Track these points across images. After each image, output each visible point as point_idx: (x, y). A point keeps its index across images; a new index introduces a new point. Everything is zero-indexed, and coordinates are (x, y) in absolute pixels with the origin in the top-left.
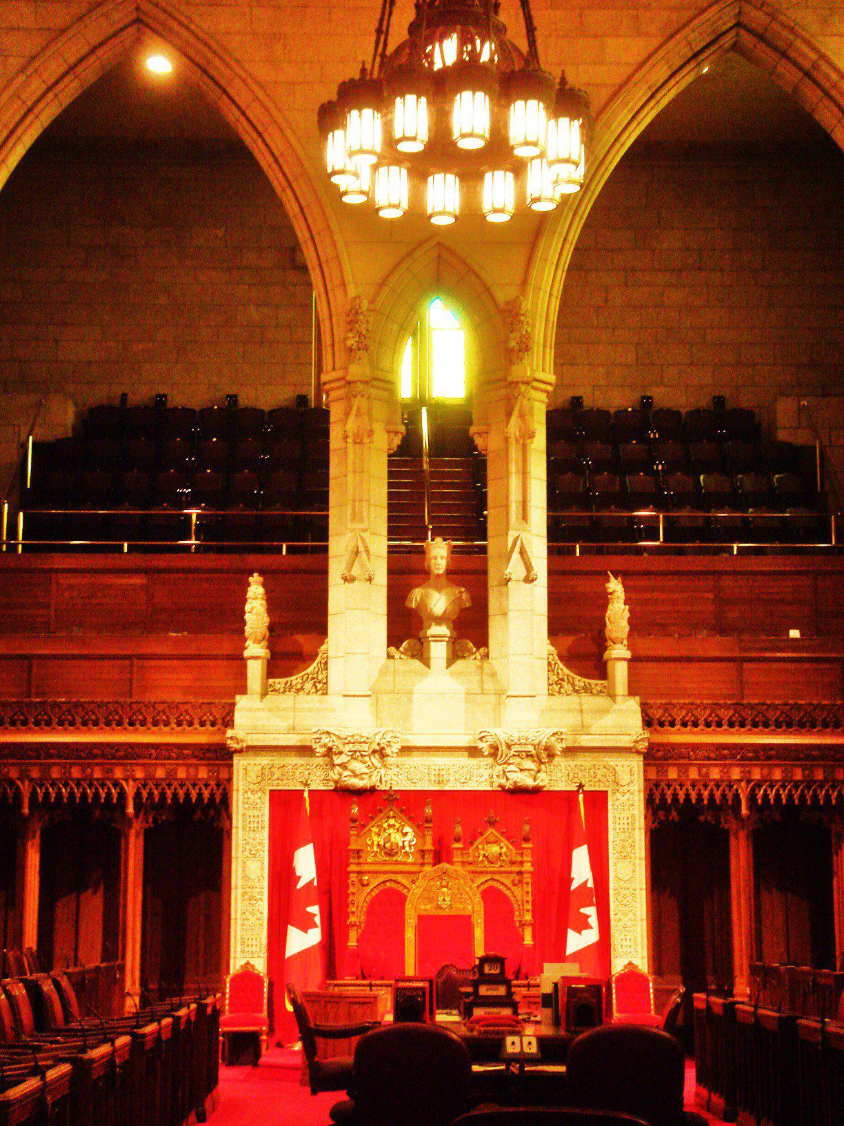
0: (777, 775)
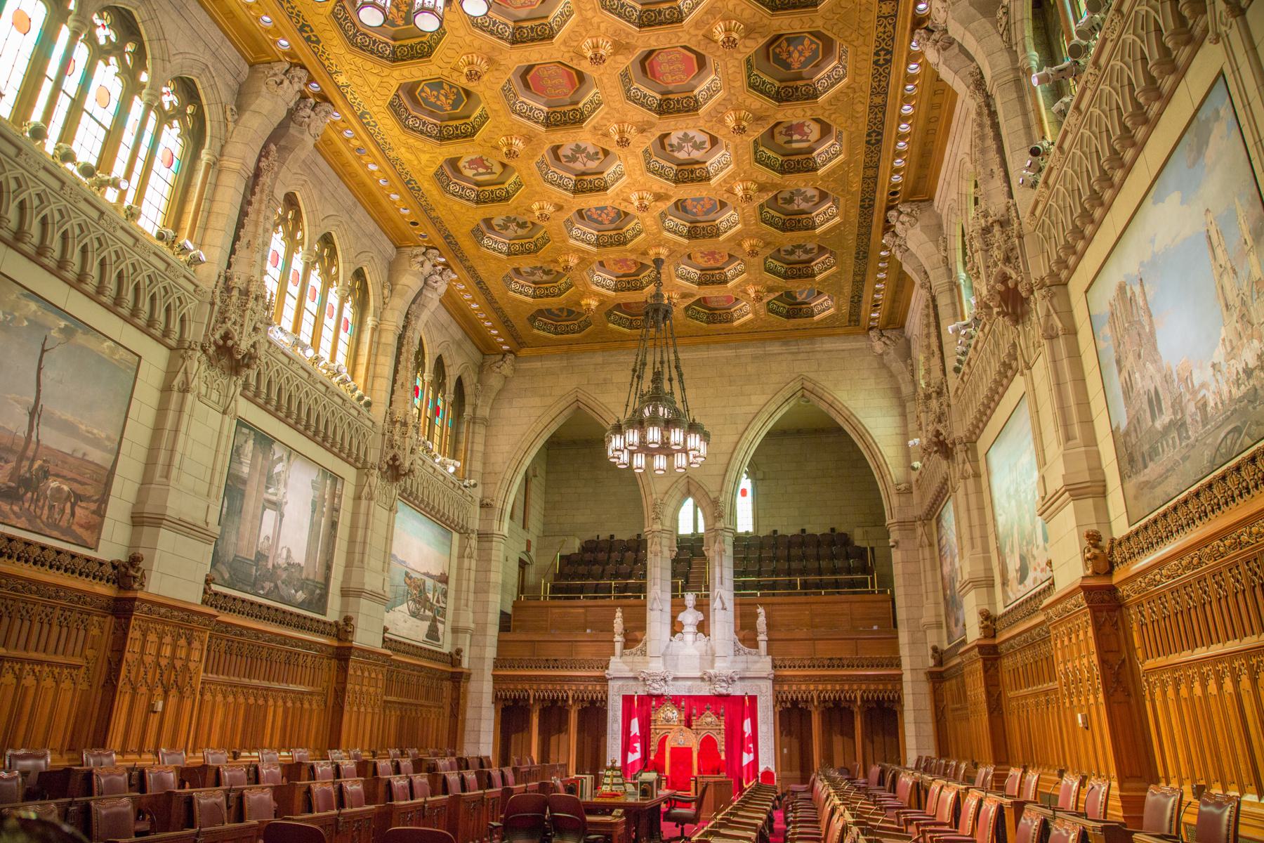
0: (829, 687)
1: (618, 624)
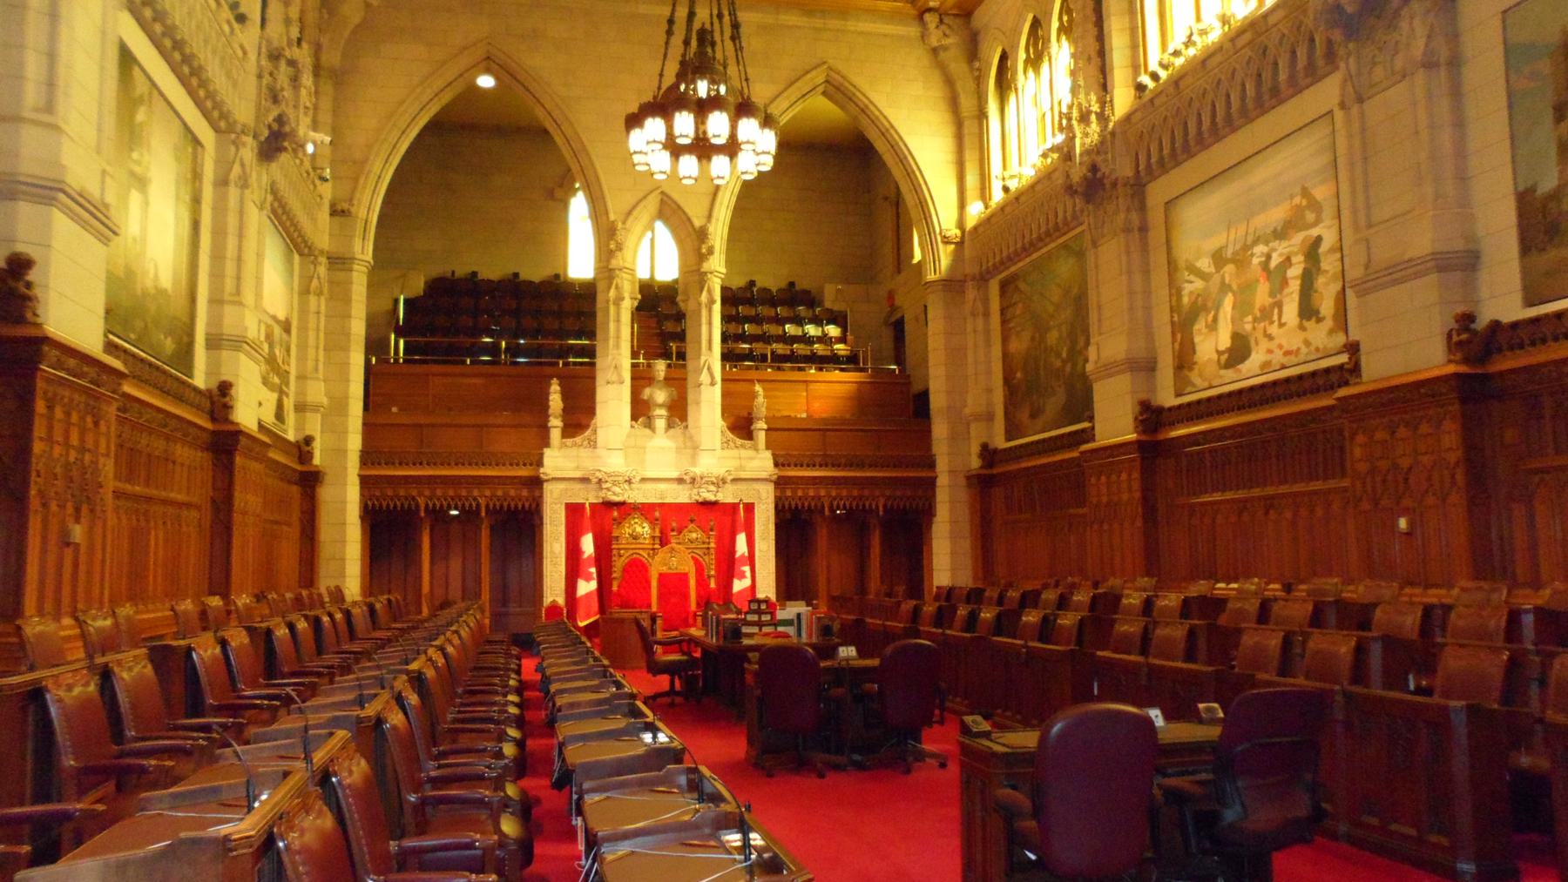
0: (844, 493)
1: (555, 400)
